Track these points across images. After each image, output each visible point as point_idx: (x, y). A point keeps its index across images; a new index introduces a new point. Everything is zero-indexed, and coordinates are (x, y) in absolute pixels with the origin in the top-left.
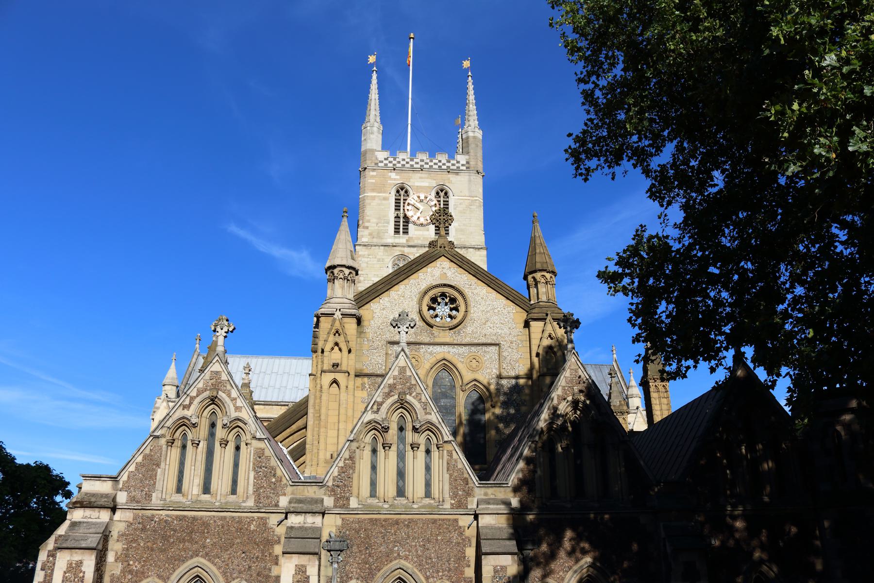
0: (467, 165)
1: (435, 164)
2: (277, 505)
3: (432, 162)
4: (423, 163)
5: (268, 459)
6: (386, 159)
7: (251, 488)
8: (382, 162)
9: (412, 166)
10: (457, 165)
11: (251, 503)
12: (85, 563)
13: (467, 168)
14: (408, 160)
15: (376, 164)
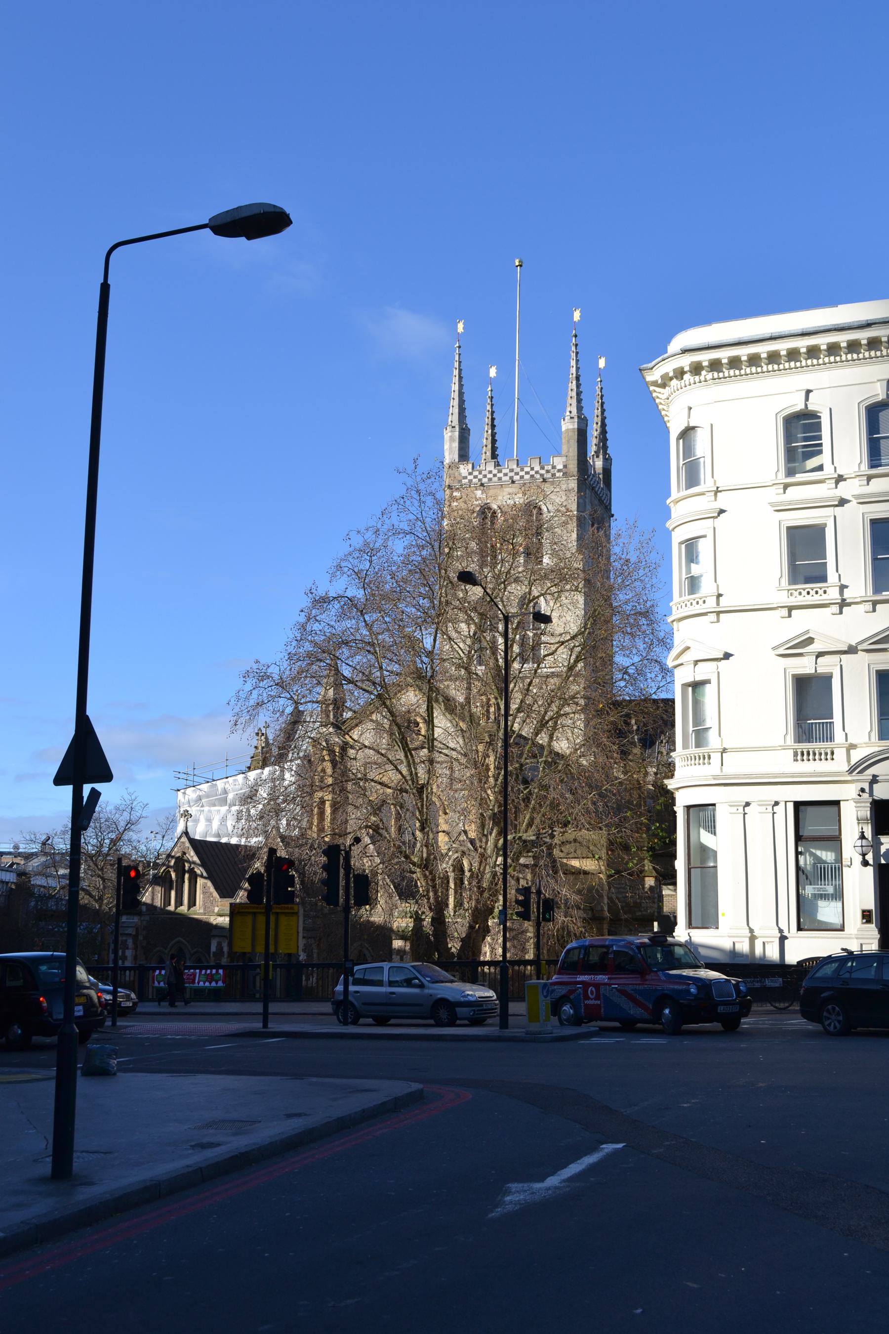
0: (564, 470)
1: (527, 473)
2: (213, 912)
3: (523, 471)
4: (512, 474)
5: (209, 888)
6: (470, 474)
7: (201, 903)
8: (465, 478)
9: (500, 479)
10: (552, 471)
11: (202, 911)
12: (128, 941)
13: (565, 474)
14: (495, 472)
15: (460, 481)
